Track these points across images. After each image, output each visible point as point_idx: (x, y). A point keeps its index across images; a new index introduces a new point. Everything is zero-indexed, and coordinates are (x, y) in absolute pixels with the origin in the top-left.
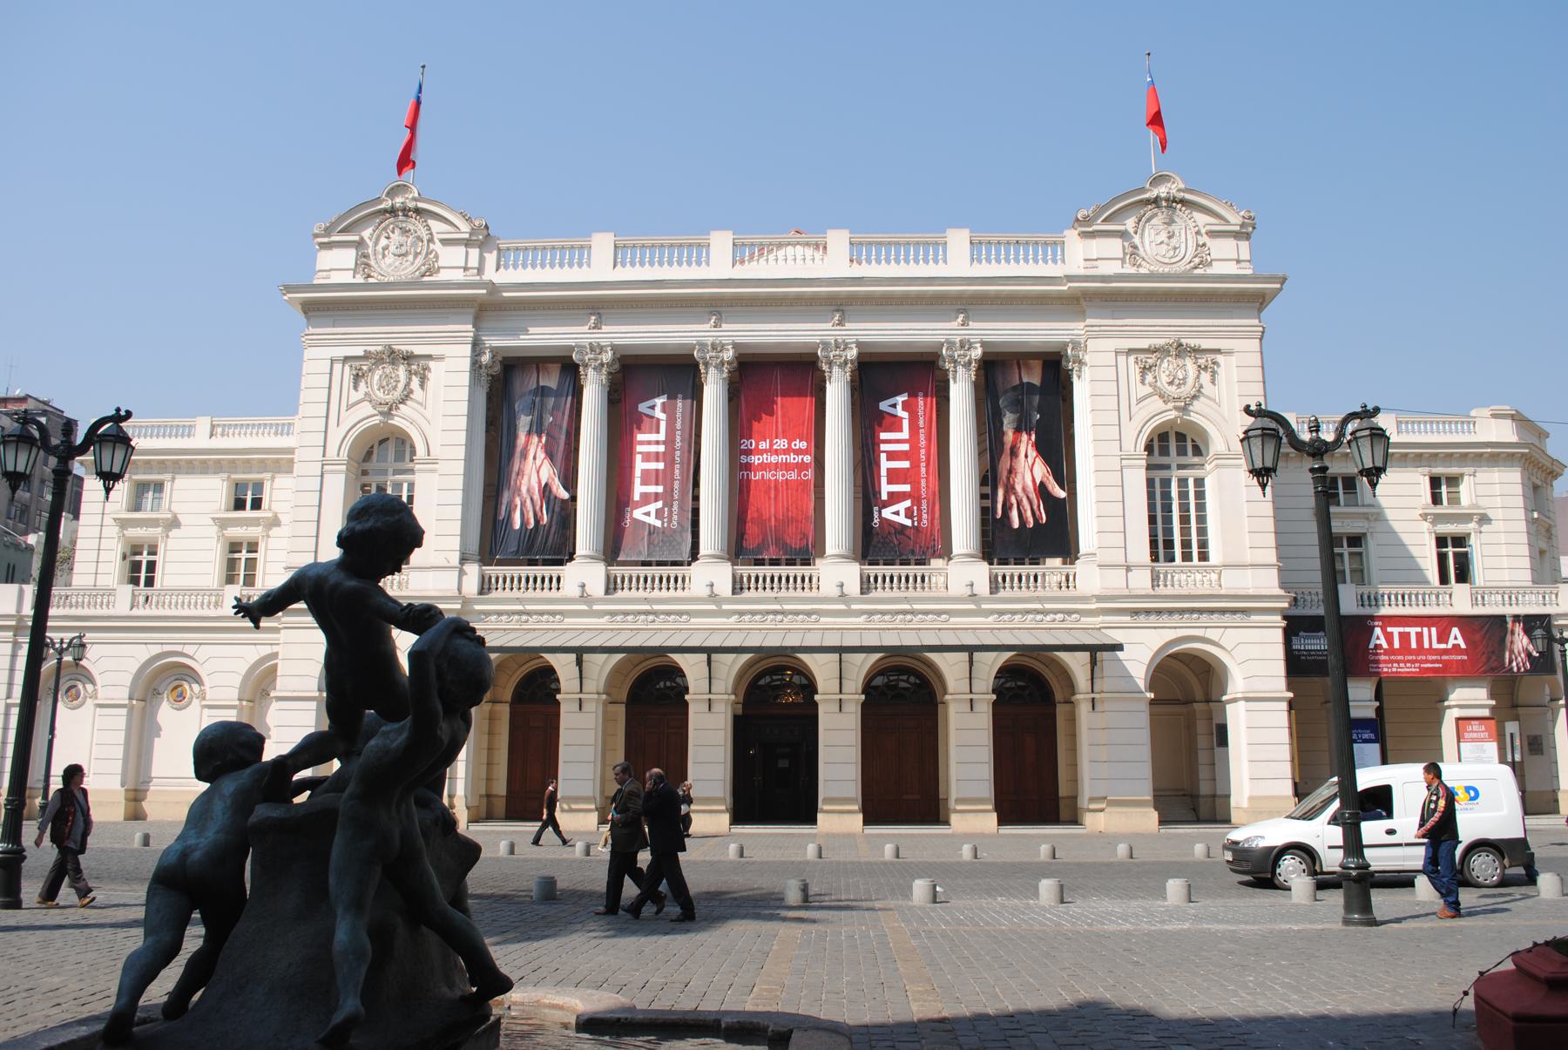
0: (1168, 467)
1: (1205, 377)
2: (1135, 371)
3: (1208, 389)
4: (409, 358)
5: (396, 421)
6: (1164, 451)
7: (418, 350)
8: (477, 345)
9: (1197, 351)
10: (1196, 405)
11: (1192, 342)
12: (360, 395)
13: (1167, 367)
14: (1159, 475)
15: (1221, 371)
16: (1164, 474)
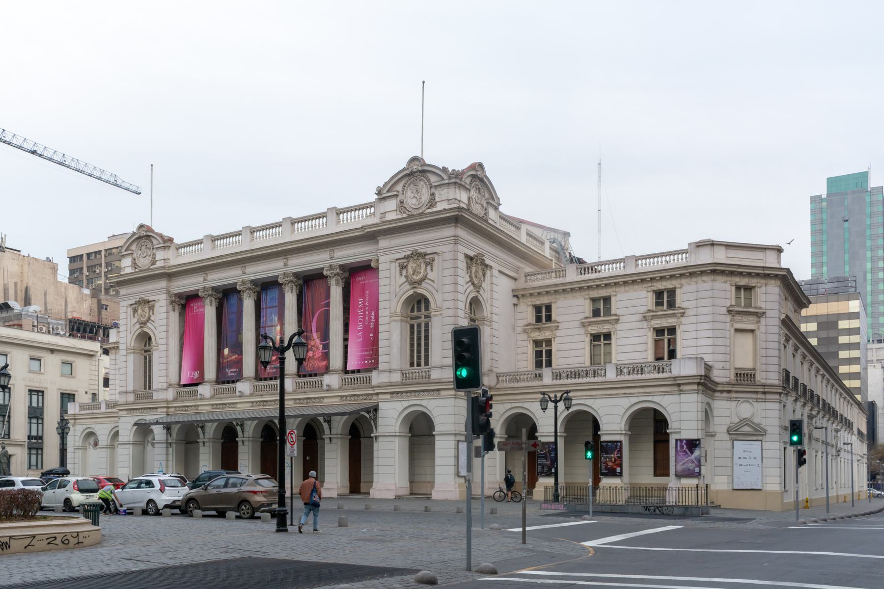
0: (419, 317)
1: (429, 267)
2: (398, 269)
3: (431, 275)
4: (149, 302)
5: (145, 330)
6: (419, 310)
7: (151, 299)
8: (168, 292)
9: (426, 254)
10: (424, 284)
11: (422, 251)
12: (135, 320)
13: (411, 265)
14: (415, 322)
15: (435, 264)
16: (418, 321)
